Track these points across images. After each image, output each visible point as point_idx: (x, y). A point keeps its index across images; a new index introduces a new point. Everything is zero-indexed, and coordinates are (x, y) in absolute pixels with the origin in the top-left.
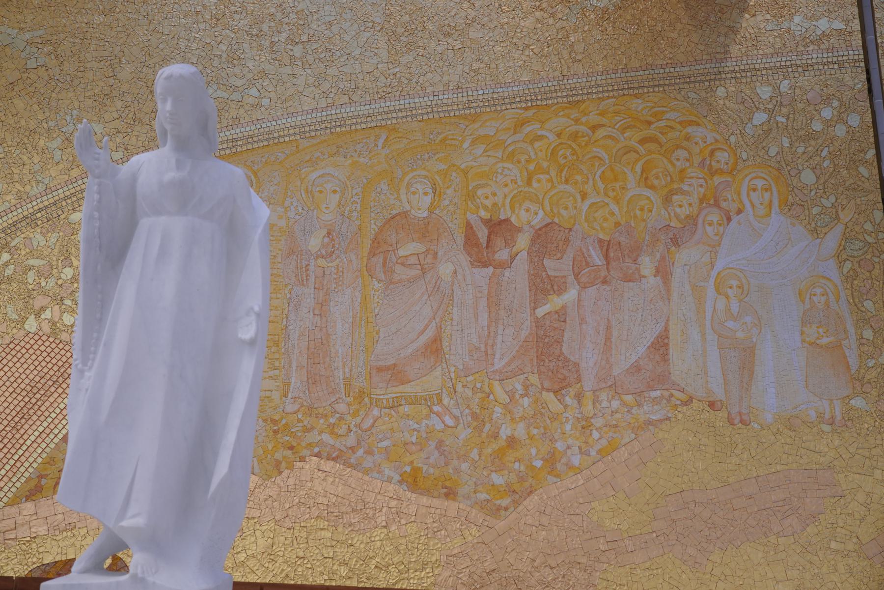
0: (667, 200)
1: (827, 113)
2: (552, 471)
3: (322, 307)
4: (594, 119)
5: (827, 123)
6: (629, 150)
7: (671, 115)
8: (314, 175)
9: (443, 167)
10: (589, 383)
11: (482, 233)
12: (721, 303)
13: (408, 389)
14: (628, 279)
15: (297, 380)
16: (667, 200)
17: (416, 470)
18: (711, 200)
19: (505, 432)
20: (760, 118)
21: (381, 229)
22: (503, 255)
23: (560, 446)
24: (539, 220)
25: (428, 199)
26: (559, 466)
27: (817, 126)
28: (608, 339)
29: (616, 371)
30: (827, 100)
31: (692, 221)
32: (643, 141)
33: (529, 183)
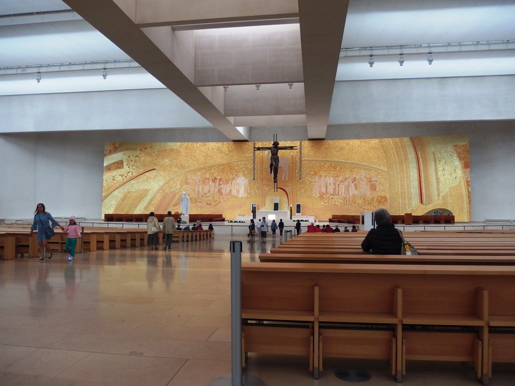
0: (232, 175)
1: (249, 165)
2: (220, 203)
3: (199, 187)
4: (225, 166)
5: (249, 166)
6: (229, 170)
7: (233, 166)
8: (197, 174)
9: (210, 172)
10: (224, 194)
11: (214, 179)
12: (237, 186)
13: (207, 195)
14: (228, 184)
15: (196, 195)
16: (232, 175)
17: (208, 203)
18: (236, 175)
19: (216, 199)
20: (242, 166)
21: (204, 179)
22: (216, 182)
23: (221, 200)
24: (219, 178)
25: (208, 176)
26: (221, 202)
27: (248, 167)
28: (226, 190)
29: (226, 193)
30: (249, 164)
31: (234, 177)
32: (230, 169)
33: (219, 174)
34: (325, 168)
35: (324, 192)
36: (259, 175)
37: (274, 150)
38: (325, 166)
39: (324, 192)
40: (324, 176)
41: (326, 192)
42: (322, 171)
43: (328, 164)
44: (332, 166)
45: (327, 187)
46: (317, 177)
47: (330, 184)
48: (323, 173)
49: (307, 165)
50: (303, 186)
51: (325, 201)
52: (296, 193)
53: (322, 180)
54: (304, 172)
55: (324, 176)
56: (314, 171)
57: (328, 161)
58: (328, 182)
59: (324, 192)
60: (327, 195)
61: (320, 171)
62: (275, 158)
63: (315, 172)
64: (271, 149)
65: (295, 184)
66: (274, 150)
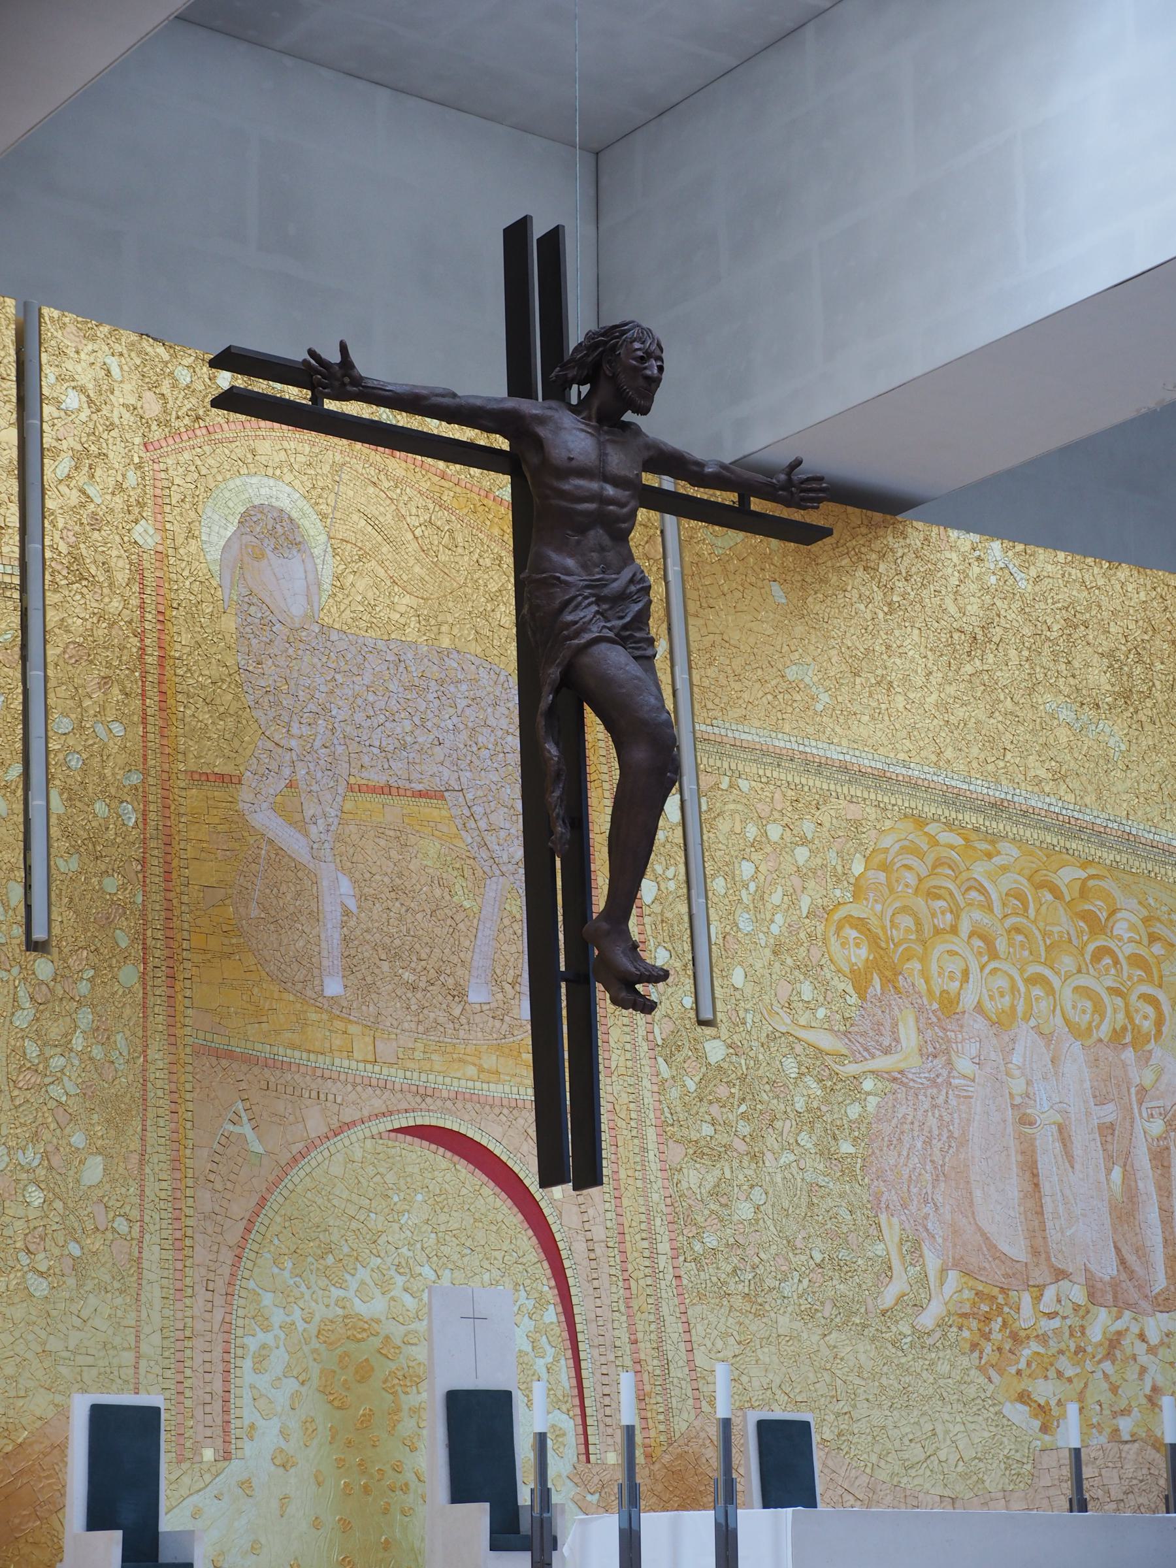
34: (990, 908)
35: (1017, 1250)
36: (111, 884)
37: (602, 456)
38: (979, 871)
39: (1017, 1250)
40: (979, 1008)
41: (1035, 1253)
42: (957, 944)
43: (1009, 852)
44: (1057, 894)
45: (1037, 1185)
46: (911, 1022)
47: (1063, 1134)
48: (966, 973)
49: (775, 832)
50: (744, 1129)
51: (1044, 1390)
52: (664, 1247)
53: (964, 1065)
54: (745, 925)
55: (979, 1008)
56: (860, 924)
57: (998, 808)
58: (1044, 1111)
59: (1005, 1248)
60: (1050, 1293)
61: (937, 932)
62: (622, 597)
63: (874, 941)
64: (542, 432)
65: (649, 1099)
66: (602, 456)
